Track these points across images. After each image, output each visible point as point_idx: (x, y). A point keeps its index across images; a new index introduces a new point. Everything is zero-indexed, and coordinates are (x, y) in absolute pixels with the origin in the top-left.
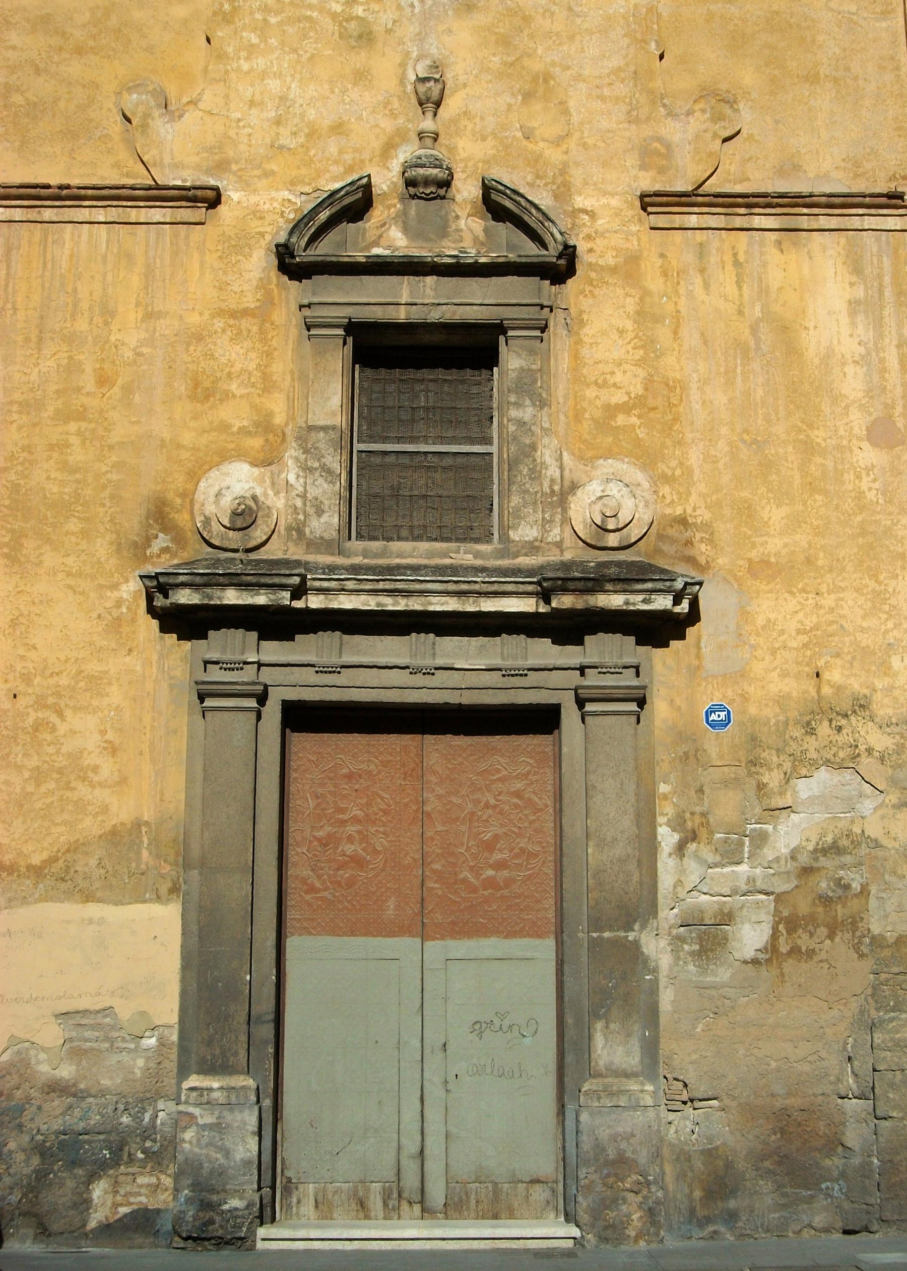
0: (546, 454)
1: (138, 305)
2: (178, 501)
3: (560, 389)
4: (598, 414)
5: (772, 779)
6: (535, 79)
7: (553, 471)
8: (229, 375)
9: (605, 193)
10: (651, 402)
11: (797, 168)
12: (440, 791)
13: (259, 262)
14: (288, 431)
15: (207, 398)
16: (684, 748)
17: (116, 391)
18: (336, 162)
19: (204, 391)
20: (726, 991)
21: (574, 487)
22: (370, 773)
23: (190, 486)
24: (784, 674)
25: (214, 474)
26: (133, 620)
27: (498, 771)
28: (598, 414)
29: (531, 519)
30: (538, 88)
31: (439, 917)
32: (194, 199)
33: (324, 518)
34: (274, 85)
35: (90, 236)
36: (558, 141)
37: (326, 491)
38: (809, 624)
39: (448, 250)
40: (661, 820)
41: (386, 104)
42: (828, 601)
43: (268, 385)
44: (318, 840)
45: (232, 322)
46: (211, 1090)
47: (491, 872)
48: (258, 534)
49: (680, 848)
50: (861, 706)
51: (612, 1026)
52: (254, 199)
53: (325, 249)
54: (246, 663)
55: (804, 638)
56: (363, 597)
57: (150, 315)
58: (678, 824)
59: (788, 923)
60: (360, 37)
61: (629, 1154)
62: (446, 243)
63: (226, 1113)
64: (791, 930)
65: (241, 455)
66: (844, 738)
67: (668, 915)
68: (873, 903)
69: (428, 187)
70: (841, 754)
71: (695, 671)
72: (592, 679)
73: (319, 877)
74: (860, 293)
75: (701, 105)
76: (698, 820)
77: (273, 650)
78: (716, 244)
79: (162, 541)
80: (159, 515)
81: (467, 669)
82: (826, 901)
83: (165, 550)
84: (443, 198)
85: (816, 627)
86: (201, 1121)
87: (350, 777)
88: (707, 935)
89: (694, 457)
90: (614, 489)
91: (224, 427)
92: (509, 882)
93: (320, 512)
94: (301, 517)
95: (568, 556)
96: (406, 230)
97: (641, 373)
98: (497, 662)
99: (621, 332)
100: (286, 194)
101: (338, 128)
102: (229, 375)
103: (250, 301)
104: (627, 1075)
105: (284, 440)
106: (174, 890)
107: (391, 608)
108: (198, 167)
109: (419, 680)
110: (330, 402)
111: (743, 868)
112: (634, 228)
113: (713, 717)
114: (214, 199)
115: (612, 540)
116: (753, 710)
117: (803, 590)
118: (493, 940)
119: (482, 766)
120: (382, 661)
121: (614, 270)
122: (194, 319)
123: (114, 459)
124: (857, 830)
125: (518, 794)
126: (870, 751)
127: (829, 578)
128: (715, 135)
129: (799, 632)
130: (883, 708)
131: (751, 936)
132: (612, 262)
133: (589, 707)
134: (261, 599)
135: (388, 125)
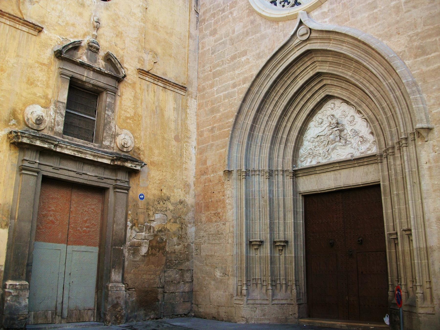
0: (112, 125)
1: (15, 51)
2: (20, 111)
3: (117, 109)
4: (124, 118)
5: (151, 213)
6: (119, 32)
7: (113, 129)
8: (38, 80)
9: (130, 65)
10: (135, 118)
11: (166, 74)
12: (75, 206)
14: (52, 100)
15: (31, 84)
16: (134, 203)
17: (6, 75)
18: (72, 33)
19: (31, 83)
20: (139, 263)
21: (118, 135)
22: (58, 198)
23: (23, 108)
24: (155, 189)
25: (31, 106)
26: (2, 143)
27: (89, 202)
28: (124, 118)
29: (108, 140)
30: (119, 35)
31: (72, 239)
32: (36, 29)
33: (59, 127)
34: (59, 7)
35: (4, 27)
36: (123, 49)
37: (61, 120)
38: (161, 178)
39: (96, 66)
40: (128, 220)
41: (86, 24)
42: (164, 174)
43: (48, 86)
44: (43, 215)
45: (40, 66)
46: (16, 285)
48: (42, 127)
49: (132, 227)
50: (168, 199)
51: (116, 270)
52: (50, 35)
54: (36, 162)
55: (159, 181)
56: (71, 151)
57: (18, 56)
58: (132, 222)
59: (151, 247)
60: (82, 4)
61: (119, 302)
62: (96, 64)
63: (20, 292)
64: (152, 249)
65: (39, 103)
66: (165, 206)
67: (128, 243)
68: (167, 244)
69: (93, 49)
70: (164, 209)
71: (138, 185)
72: (119, 183)
73: (42, 225)
74: (175, 107)
75: (150, 53)
76: (136, 221)
78: (151, 86)
79: (13, 122)
80: (14, 114)
81: (90, 175)
82: (158, 242)
83: (14, 124)
84: (97, 53)
85: (162, 179)
86: (13, 294)
87: (52, 198)
88: (135, 248)
89: (142, 134)
90: (127, 137)
91: (35, 94)
92: (89, 231)
93: (58, 125)
94: (53, 125)
95: (115, 151)
96: (87, 57)
97: (134, 111)
98: (97, 175)
99: (130, 100)
100: (59, 37)
101: (73, 25)
102: (38, 80)
103: (46, 62)
104: (118, 282)
105: (50, 103)
106: (7, 225)
107: (77, 155)
108: (37, 20)
109: (78, 176)
110: (64, 97)
111: (143, 234)
112: (136, 76)
113: (141, 197)
114: (39, 30)
115: (125, 150)
116: (148, 196)
117: (160, 170)
118: (84, 247)
119: (85, 201)
120: (70, 169)
121: (130, 84)
122: (30, 61)
123: (2, 94)
124: (165, 227)
125: (93, 209)
126: (169, 209)
127: (165, 168)
128: (153, 61)
129: (159, 180)
130: (172, 200)
131: (144, 250)
132: (130, 82)
134: (46, 146)
135: (86, 30)
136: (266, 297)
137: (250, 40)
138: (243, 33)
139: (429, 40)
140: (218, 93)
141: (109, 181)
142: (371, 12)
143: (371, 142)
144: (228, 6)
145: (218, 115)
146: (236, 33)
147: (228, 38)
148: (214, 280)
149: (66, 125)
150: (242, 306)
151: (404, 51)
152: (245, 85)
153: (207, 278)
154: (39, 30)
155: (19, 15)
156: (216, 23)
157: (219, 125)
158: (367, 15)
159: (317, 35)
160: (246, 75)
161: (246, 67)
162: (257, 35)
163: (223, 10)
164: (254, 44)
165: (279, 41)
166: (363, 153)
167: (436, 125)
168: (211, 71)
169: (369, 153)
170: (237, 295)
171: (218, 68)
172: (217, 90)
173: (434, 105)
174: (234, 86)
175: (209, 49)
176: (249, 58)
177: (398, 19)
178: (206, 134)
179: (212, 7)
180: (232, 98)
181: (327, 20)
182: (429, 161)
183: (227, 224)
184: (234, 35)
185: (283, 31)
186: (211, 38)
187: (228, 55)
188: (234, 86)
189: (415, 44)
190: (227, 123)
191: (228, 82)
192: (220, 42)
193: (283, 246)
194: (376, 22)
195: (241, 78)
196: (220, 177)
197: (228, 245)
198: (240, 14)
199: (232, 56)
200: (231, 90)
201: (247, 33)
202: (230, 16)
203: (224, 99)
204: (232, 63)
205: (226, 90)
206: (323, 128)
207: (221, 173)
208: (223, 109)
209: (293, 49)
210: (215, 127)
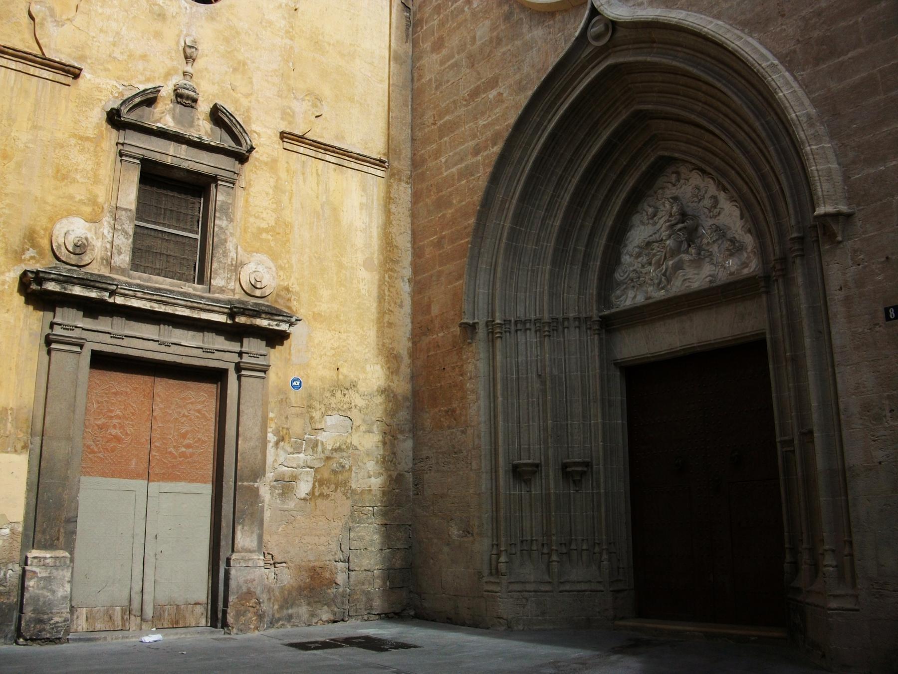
0: (230, 245)
1: (29, 119)
2: (42, 232)
3: (239, 215)
4: (255, 231)
5: (317, 415)
6: (239, 62)
7: (233, 254)
8: (76, 170)
9: (265, 126)
10: (277, 230)
11: (343, 138)
12: (162, 406)
13: (97, 116)
14: (106, 206)
15: (63, 179)
16: (281, 397)
17: (12, 165)
18: (142, 74)
19: (62, 176)
20: (294, 513)
21: (242, 264)
22: (126, 393)
23: (49, 225)
24: (324, 367)
25: (64, 221)
26: (11, 294)
27: (190, 398)
28: (255, 231)
29: (222, 276)
30: (240, 67)
31: (157, 470)
32: (68, 72)
33: (122, 257)
34: (114, 25)
35: (5, 74)
36: (247, 96)
37: (125, 243)
38: (336, 345)
39: (193, 134)
40: (269, 430)
41: (169, 53)
42: (344, 336)
43: (96, 181)
44: (98, 426)
45: (80, 142)
46: (45, 558)
47: (184, 449)
48: (86, 259)
49: (277, 444)
50: (354, 385)
51: (245, 528)
52: (97, 81)
53: (132, 117)
54: (76, 327)
55: (333, 352)
56: (144, 302)
57: (35, 127)
58: (276, 433)
59: (320, 482)
60: (159, 15)
61: (252, 590)
62: (192, 130)
63: (54, 571)
64: (320, 486)
65: (78, 214)
66: (346, 399)
67: (270, 475)
68: (353, 474)
69: (185, 99)
70: (345, 407)
71: (288, 361)
73: (97, 445)
74: (364, 201)
75: (307, 98)
76: (285, 431)
77: (89, 323)
78: (310, 163)
79: (31, 253)
80: (31, 238)
81: (186, 346)
82: (335, 472)
83: (32, 258)
84: (193, 107)
85: (338, 347)
86: (39, 575)
87: (116, 394)
88: (285, 485)
89: (294, 260)
90: (260, 268)
91: (71, 197)
92: (192, 455)
93: (120, 253)
94: (109, 254)
95: (237, 297)
96: (174, 118)
97: (275, 216)
98: (201, 344)
99: (267, 194)
100: (115, 83)
101: (144, 57)
102: (76, 170)
103: (91, 133)
104: (250, 551)
105: (102, 211)
106: (24, 447)
108: (69, 55)
109: (163, 348)
110: (129, 196)
111: (302, 455)
112: (276, 146)
113: (294, 383)
114: (75, 74)
115: (258, 293)
116: (311, 382)
117: (334, 330)
118: (183, 484)
119: (183, 395)
120: (146, 336)
121: (266, 164)
122: (59, 135)
123: (8, 201)
124: (349, 442)
125: (199, 411)
126: (356, 406)
127: (345, 326)
128: (313, 113)
129: (332, 349)
130: (362, 387)
131: (304, 488)
132: (265, 159)
133: (243, 372)
134: (93, 294)
135: (169, 64)
136: (547, 578)
137: (504, 54)
138: (491, 41)
139: (843, 24)
140: (448, 168)
141: (227, 356)
145: (449, 212)
146: (478, 43)
147: (463, 55)
148: (448, 545)
149: (136, 251)
151: (795, 51)
153: (435, 541)
154: (75, 74)
155: (37, 51)
156: (442, 24)
160: (497, 128)
161: (498, 110)
162: (516, 42)
164: (510, 61)
165: (556, 51)
168: (435, 124)
170: (491, 574)
171: (447, 118)
172: (446, 161)
173: (854, 162)
174: (476, 151)
175: (430, 80)
178: (428, 252)
180: (473, 175)
183: (470, 431)
184: (475, 47)
185: (564, 30)
186: (435, 57)
189: (816, 34)
192: (449, 63)
193: (583, 474)
195: (489, 134)
196: (455, 336)
200: (470, 160)
201: (499, 41)
202: (466, 9)
203: (459, 180)
204: (473, 104)
205: (462, 160)
206: (658, 226)
208: (458, 198)
209: (583, 68)
210: (443, 237)
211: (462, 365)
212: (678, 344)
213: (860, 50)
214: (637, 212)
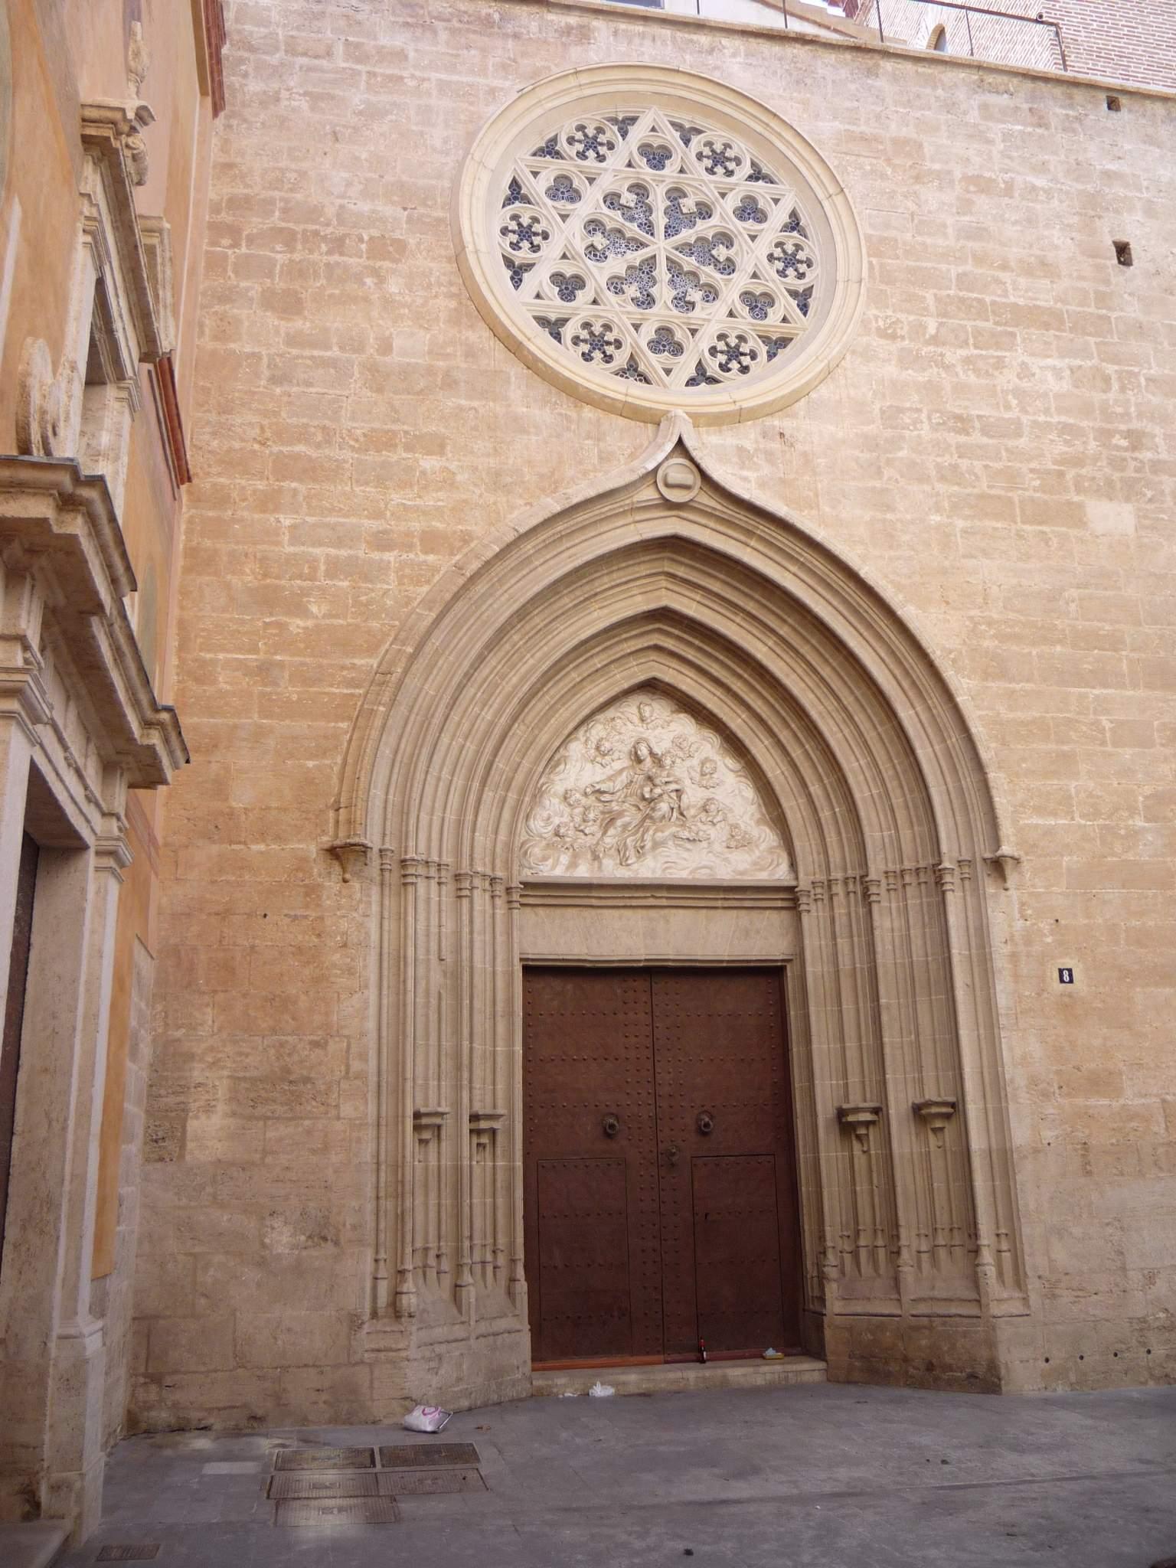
137: (461, 408)
138: (430, 371)
139: (1014, 648)
142: (879, 516)
143: (763, 847)
144: (361, 240)
145: (297, 625)
146: (395, 359)
150: (404, 1354)
152: (431, 558)
157: (303, 664)
158: (867, 518)
159: (719, 507)
163: (338, 245)
164: (475, 428)
165: (580, 463)
166: (741, 873)
167: (1027, 854)
169: (763, 877)
171: (300, 448)
173: (1022, 805)
174: (381, 541)
176: (453, 466)
177: (947, 563)
179: (280, 205)
180: (371, 581)
181: (752, 475)
182: (1012, 940)
183: (333, 1046)
184: (387, 359)
186: (272, 319)
187: (353, 419)
188: (381, 541)
189: (986, 643)
190: (343, 668)
191: (354, 520)
192: (316, 353)
194: (891, 547)
195: (416, 525)
197: (338, 1126)
198: (419, 301)
199: (373, 430)
200: (361, 552)
201: (450, 383)
202: (369, 281)
205: (339, 543)
206: (608, 771)
207: (312, 849)
208: (325, 608)
211: (322, 918)
212: (642, 951)
213: (1029, 686)
214: (577, 739)
